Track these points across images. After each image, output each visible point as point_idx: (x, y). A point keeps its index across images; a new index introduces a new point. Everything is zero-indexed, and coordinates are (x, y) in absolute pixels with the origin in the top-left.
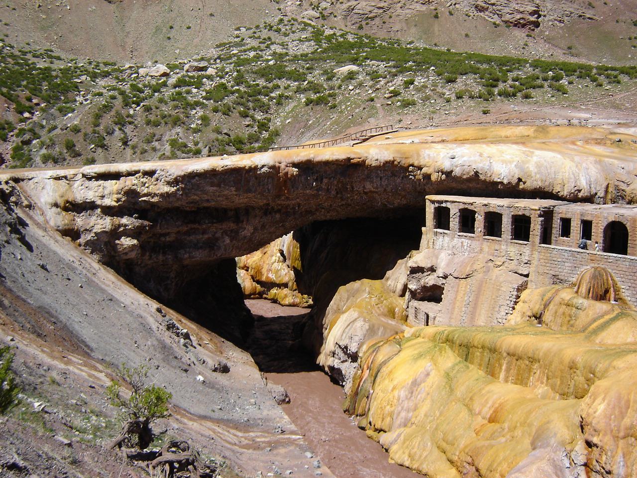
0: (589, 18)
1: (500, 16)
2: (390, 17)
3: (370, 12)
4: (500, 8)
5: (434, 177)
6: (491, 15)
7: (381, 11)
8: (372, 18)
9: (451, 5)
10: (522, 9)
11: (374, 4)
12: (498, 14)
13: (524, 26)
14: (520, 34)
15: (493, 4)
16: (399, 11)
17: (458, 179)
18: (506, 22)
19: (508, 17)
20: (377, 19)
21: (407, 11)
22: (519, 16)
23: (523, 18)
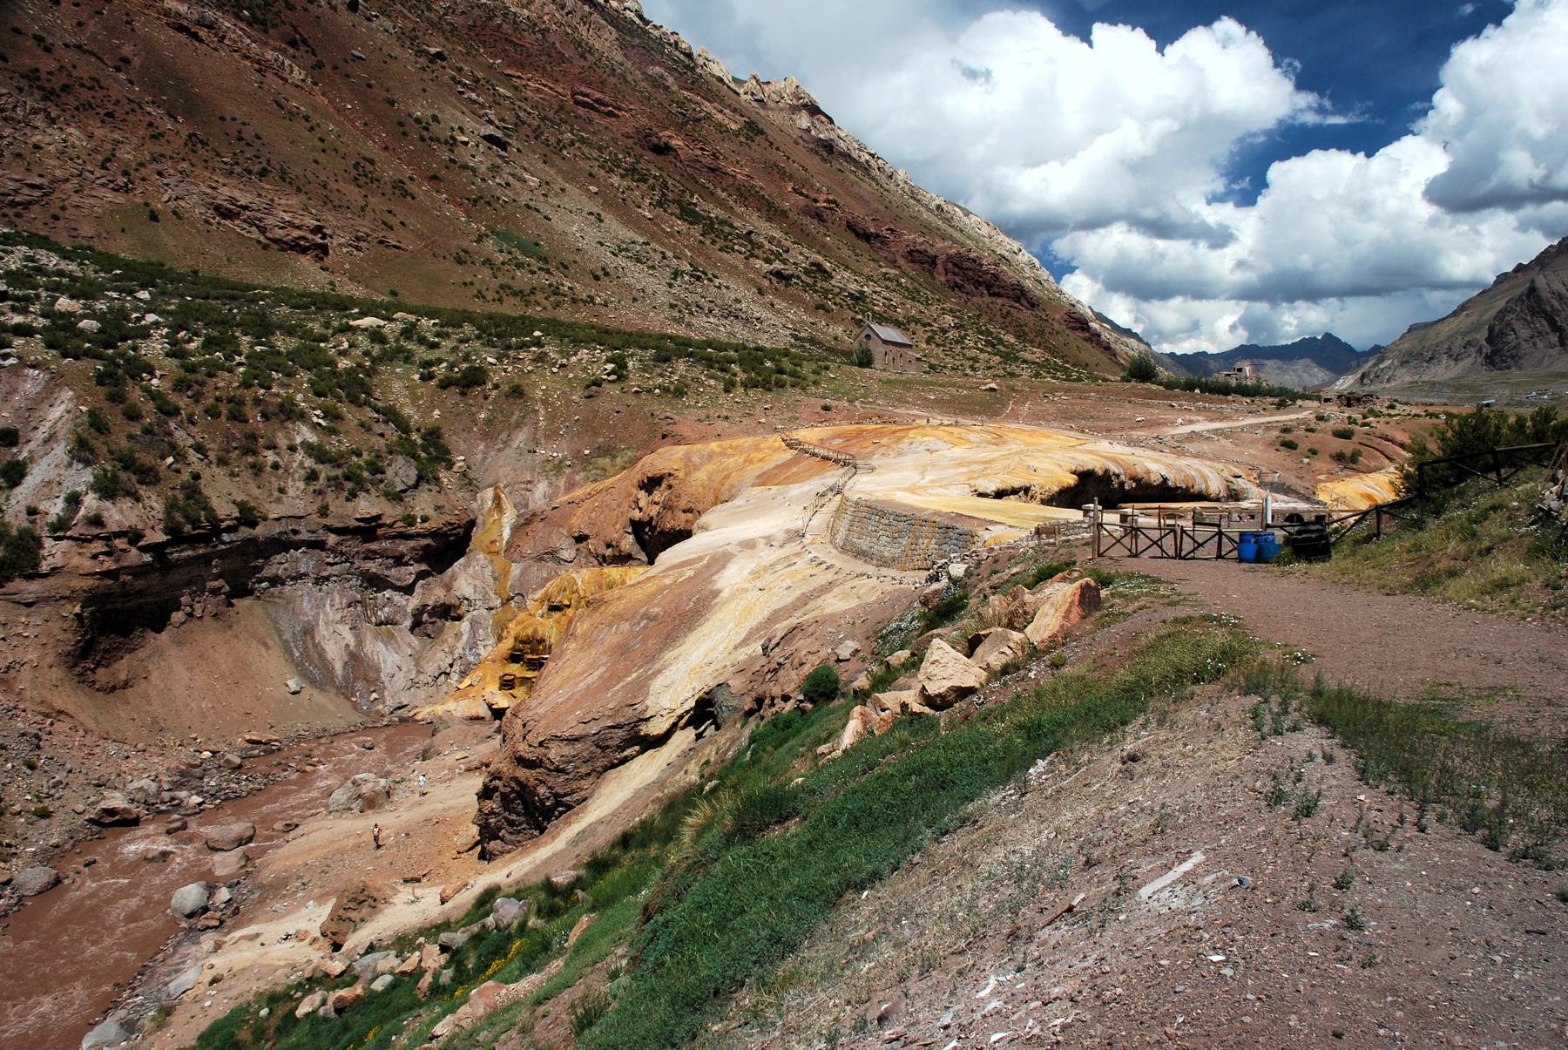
0: (395, 247)
1: (263, 230)
2: (63, 208)
3: (16, 191)
4: (259, 215)
5: (1126, 487)
6: (245, 226)
7: (38, 193)
8: (27, 205)
9: (169, 200)
10: (297, 222)
11: (18, 177)
12: (257, 226)
13: (304, 251)
14: (306, 262)
15: (245, 208)
16: (76, 199)
17: (1149, 486)
18: (275, 241)
19: (278, 233)
20: (36, 208)
21: (92, 201)
22: (296, 233)
23: (303, 238)
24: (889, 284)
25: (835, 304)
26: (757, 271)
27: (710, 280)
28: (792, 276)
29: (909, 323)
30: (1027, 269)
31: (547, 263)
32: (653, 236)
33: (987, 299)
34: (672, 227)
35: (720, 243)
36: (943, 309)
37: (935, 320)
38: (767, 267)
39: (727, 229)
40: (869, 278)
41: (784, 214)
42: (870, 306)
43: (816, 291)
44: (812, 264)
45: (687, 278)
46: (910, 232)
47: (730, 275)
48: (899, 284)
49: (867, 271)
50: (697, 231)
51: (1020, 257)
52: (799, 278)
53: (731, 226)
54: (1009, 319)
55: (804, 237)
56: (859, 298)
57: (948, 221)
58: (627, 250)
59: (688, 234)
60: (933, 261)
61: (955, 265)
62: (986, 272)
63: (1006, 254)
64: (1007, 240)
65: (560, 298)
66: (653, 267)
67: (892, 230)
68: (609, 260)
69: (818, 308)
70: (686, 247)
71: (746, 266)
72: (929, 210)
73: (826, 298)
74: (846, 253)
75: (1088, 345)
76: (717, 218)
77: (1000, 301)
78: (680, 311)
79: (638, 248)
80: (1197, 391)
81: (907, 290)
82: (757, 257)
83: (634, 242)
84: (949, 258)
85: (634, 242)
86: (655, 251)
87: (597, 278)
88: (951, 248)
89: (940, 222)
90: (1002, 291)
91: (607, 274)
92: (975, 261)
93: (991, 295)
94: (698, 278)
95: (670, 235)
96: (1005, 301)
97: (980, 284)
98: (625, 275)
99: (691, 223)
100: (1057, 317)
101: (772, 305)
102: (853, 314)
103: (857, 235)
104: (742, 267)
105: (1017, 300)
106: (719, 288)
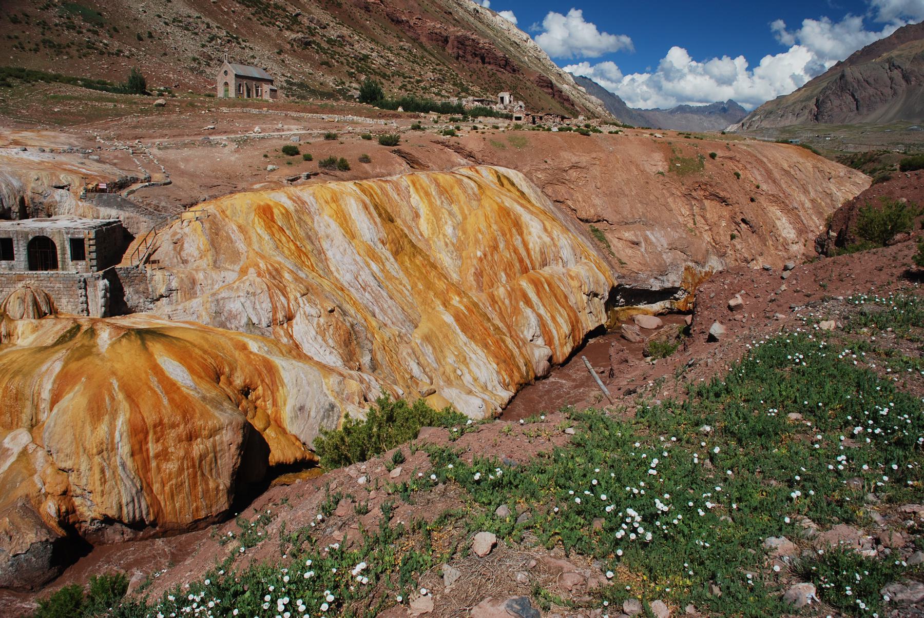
24: (403, 52)
25: (337, 62)
26: (285, 39)
27: (239, 43)
28: (314, 42)
29: (393, 76)
30: (532, 52)
31: (102, 27)
32: (210, 14)
33: (480, 65)
34: (229, 8)
35: (266, 20)
36: (435, 69)
37: (421, 75)
38: (294, 36)
39: (280, 11)
40: (388, 49)
41: (339, 5)
42: (369, 64)
43: (325, 53)
44: (339, 37)
45: (219, 41)
46: (432, 20)
47: (263, 40)
48: (410, 52)
49: (389, 44)
50: (248, 12)
51: (528, 44)
52: (318, 45)
53: (284, 10)
54: (492, 78)
55: (348, 20)
56: (366, 58)
57: (481, 21)
58: (180, 22)
59: (241, 14)
60: (446, 40)
61: (458, 42)
62: (480, 49)
63: (518, 41)
64: (520, 32)
65: (90, 51)
66: (196, 34)
67: (420, 19)
68: (158, 26)
69: (322, 64)
70: (235, 21)
71: (278, 35)
72: (466, 10)
73: (332, 58)
74: (378, 31)
75: (549, 97)
76: (275, 4)
77: (489, 67)
78: (199, 63)
79: (191, 20)
80: (400, 109)
81: (415, 56)
82: (292, 30)
83: (189, 17)
84: (457, 37)
85: (189, 17)
86: (203, 22)
87: (140, 39)
88: (458, 32)
89: (472, 19)
90: (492, 61)
91: (150, 36)
92: (473, 40)
93: (484, 63)
94: (229, 41)
95: (227, 13)
96: (494, 67)
97: (476, 55)
98: (168, 38)
99: (248, 6)
100: (532, 78)
101: (283, 61)
102: (347, 68)
103: (393, 20)
104: (274, 36)
105: (505, 67)
106: (243, 48)
